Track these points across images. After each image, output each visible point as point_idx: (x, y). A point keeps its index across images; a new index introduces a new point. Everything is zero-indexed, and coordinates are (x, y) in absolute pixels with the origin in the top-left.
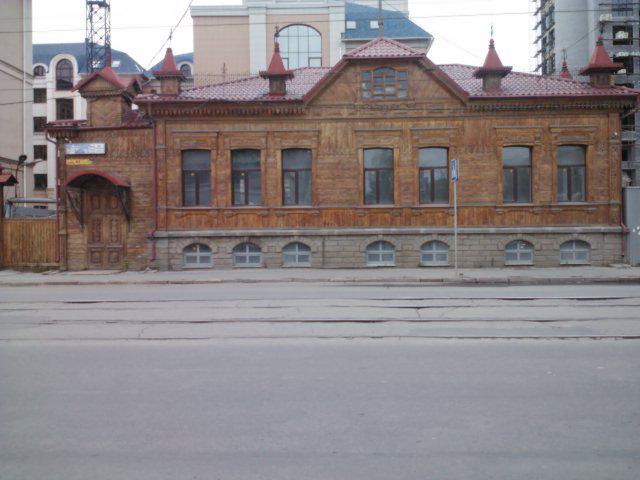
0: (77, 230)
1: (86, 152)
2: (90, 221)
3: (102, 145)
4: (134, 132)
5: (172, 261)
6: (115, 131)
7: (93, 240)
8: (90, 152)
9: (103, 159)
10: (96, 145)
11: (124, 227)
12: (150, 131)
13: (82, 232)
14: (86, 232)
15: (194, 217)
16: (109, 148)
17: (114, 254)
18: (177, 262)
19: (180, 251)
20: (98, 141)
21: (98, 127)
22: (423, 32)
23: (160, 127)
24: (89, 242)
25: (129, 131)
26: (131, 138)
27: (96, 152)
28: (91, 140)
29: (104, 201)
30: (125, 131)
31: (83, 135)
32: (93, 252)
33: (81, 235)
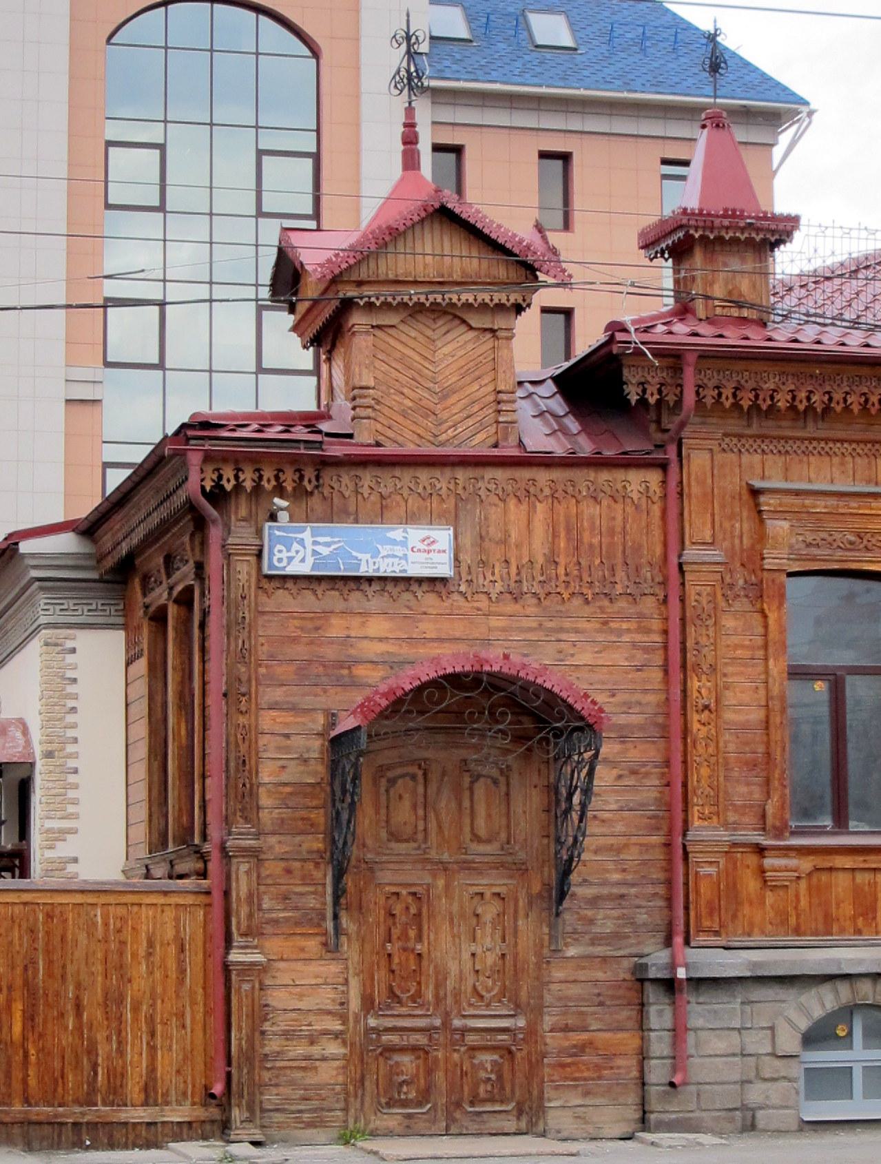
0: (313, 945)
1: (365, 570)
2: (375, 899)
3: (443, 536)
4: (584, 478)
5: (755, 1094)
6: (500, 474)
7: (392, 994)
8: (387, 568)
9: (429, 600)
10: (415, 534)
11: (529, 929)
12: (654, 477)
13: (331, 948)
14: (350, 950)
15: (842, 882)
16: (466, 558)
17: (487, 1058)
18: (775, 1092)
19: (789, 1042)
20: (410, 518)
21: (410, 449)
22: (767, 83)
23: (698, 461)
24: (368, 1003)
25: (557, 474)
26: (561, 509)
27: (416, 568)
28: (382, 513)
29: (445, 803)
30: (543, 477)
31: (345, 481)
32: (391, 1049)
33: (334, 968)
